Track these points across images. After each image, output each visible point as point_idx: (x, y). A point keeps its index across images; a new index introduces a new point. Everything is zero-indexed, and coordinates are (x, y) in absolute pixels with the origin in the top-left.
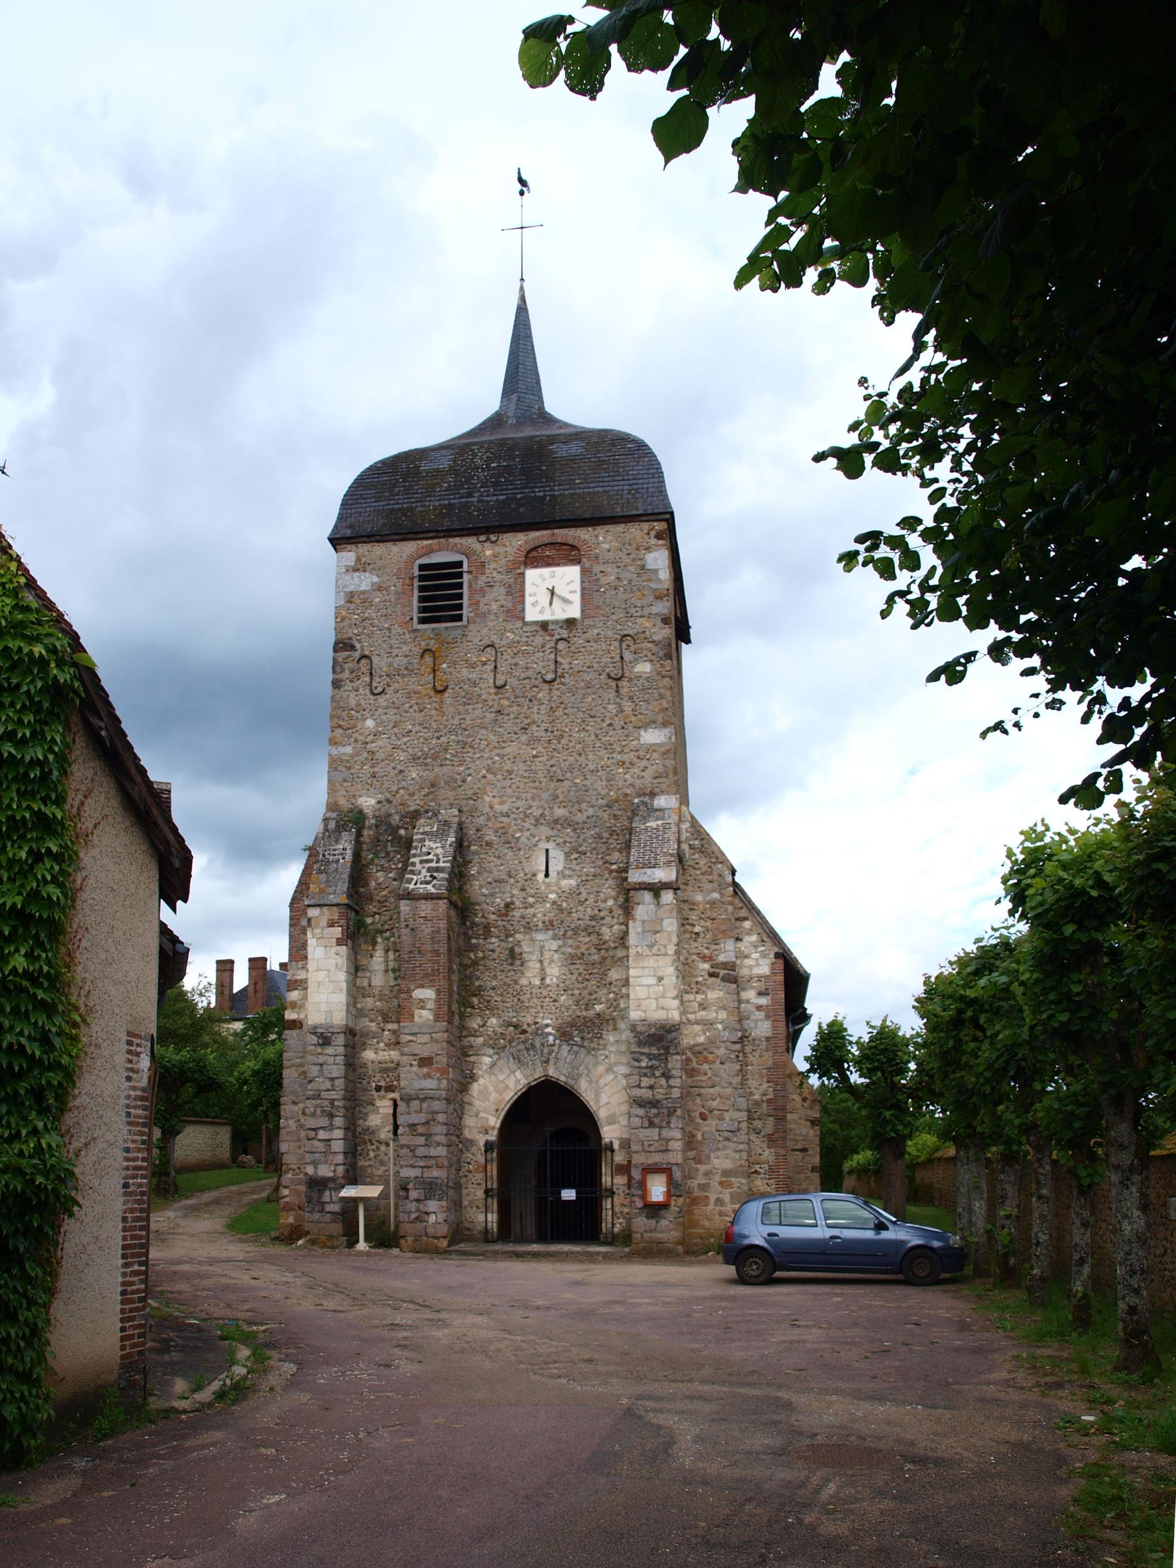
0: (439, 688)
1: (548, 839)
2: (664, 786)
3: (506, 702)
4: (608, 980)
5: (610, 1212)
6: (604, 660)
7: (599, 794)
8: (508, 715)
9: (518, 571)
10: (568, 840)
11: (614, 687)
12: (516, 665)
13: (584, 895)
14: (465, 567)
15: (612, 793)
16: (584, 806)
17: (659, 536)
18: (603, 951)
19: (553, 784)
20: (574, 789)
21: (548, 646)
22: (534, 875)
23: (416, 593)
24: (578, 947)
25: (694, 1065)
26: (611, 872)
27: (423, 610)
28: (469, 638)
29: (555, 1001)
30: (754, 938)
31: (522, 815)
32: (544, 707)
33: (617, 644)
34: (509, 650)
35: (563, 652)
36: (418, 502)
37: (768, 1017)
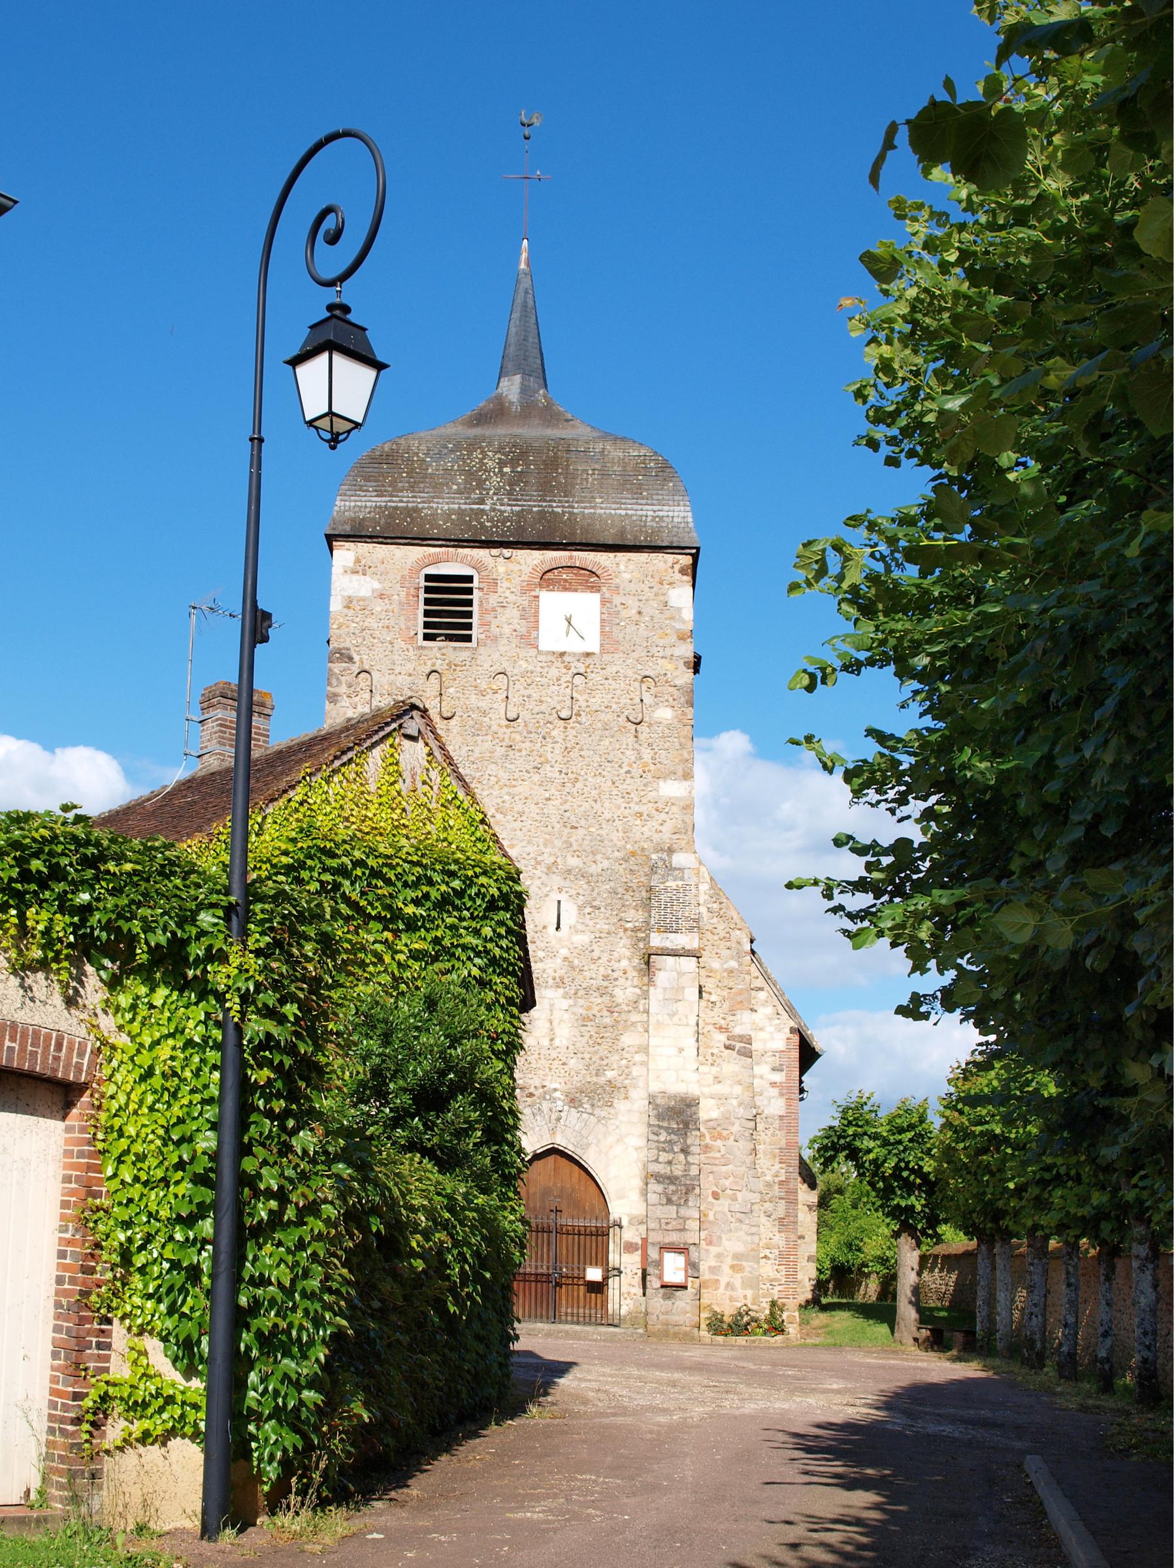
0: (445, 715)
1: (560, 890)
2: (683, 843)
3: (518, 737)
4: (621, 1045)
5: (617, 1292)
6: (623, 701)
7: (615, 845)
8: (520, 751)
9: (533, 593)
10: (582, 892)
11: (633, 731)
12: (529, 697)
13: (596, 954)
14: (475, 584)
15: (628, 846)
16: (599, 857)
17: (683, 571)
18: (616, 1014)
19: (567, 830)
20: (589, 838)
21: (564, 679)
22: (545, 927)
23: (422, 607)
24: (589, 1008)
25: (708, 1140)
26: (626, 930)
27: (427, 625)
28: (479, 662)
29: (564, 1064)
30: (769, 1010)
31: (533, 862)
32: (557, 746)
33: (637, 684)
34: (522, 680)
35: (580, 688)
36: (423, 502)
37: (781, 1095)
